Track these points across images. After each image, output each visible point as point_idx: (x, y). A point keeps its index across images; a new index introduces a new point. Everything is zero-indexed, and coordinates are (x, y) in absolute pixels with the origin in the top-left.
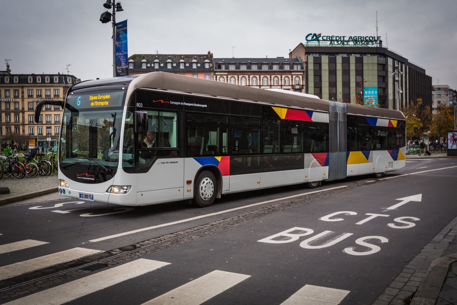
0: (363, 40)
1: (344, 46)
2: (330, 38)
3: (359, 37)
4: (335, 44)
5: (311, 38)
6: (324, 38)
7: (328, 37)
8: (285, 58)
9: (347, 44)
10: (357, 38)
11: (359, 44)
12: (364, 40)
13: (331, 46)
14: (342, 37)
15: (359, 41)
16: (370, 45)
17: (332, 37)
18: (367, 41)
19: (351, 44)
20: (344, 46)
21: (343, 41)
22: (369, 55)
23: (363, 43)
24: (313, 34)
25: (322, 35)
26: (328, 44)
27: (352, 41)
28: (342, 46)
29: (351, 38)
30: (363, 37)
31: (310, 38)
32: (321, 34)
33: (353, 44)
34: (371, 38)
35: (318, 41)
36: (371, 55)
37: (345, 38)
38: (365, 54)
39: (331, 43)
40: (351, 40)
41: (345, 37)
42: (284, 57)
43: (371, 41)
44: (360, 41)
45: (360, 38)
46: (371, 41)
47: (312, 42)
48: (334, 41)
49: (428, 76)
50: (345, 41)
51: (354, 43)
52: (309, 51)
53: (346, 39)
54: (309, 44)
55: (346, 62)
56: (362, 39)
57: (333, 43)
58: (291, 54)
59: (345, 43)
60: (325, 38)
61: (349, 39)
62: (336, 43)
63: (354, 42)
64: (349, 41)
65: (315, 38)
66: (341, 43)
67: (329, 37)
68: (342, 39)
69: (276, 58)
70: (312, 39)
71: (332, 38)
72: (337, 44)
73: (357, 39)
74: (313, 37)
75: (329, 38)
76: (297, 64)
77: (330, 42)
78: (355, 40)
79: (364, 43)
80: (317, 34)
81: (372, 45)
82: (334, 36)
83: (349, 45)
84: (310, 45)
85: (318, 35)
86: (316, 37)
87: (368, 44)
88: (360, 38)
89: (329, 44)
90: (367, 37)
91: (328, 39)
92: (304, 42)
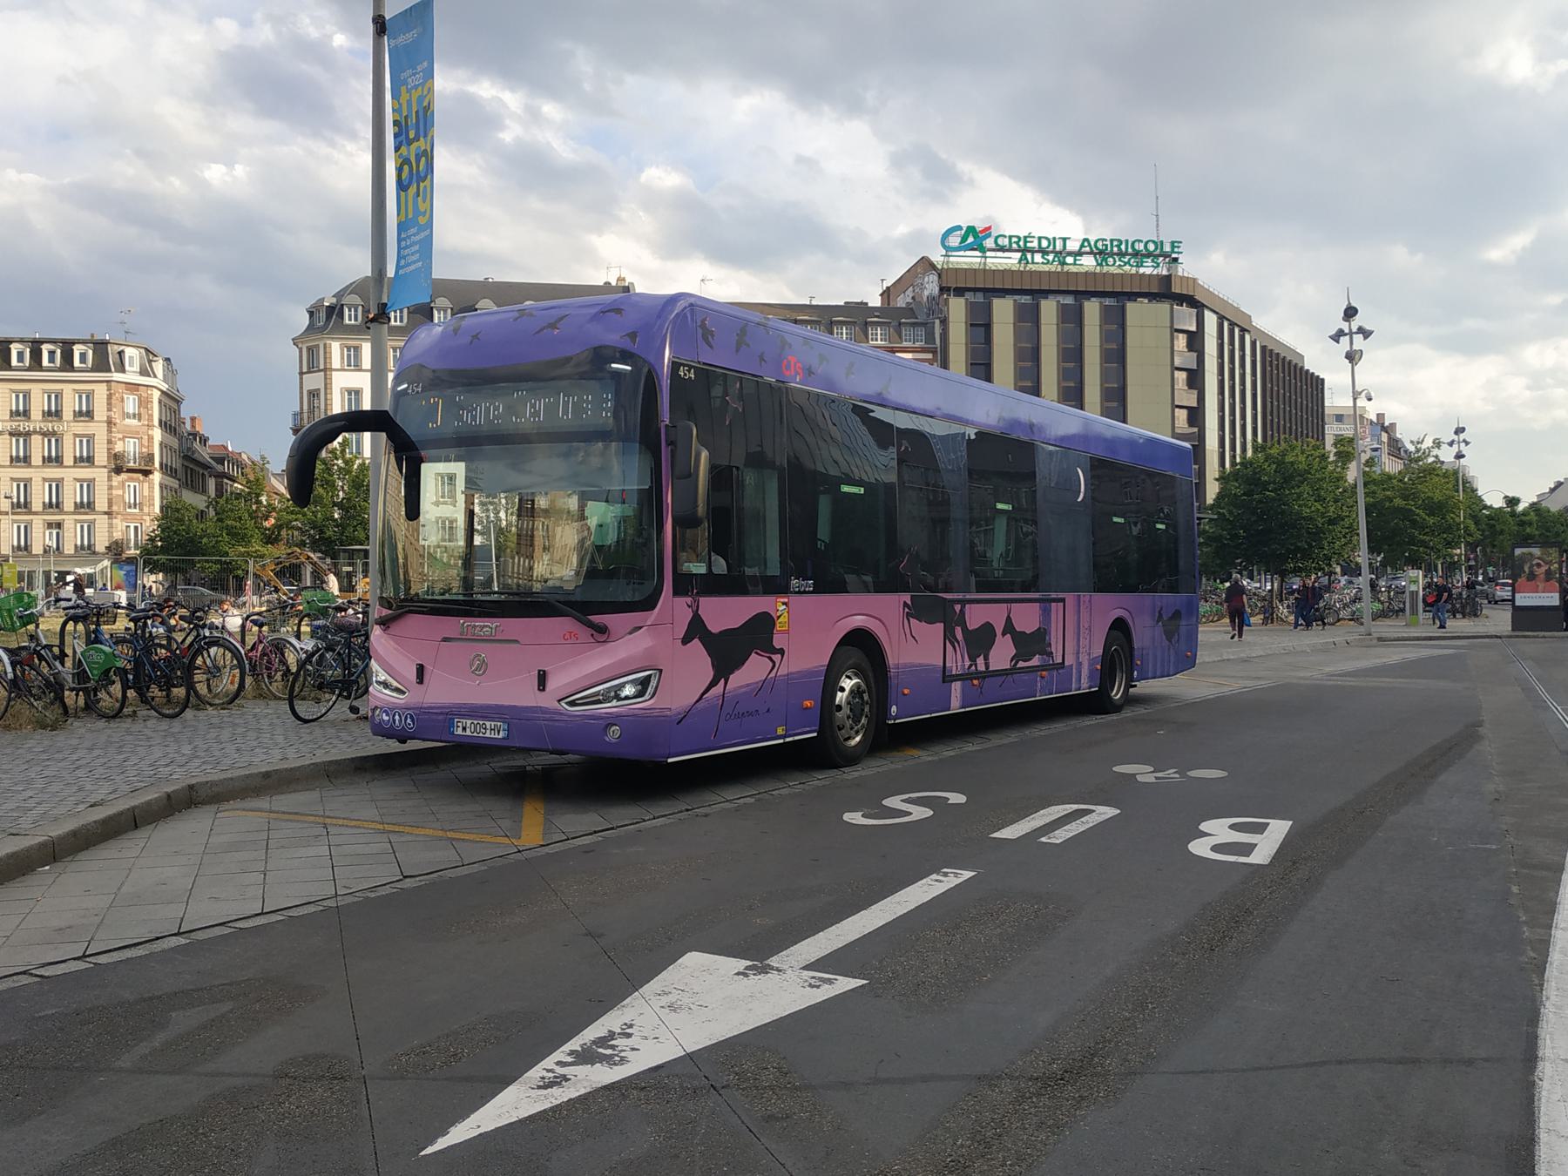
0: (1126, 254)
1: (1066, 268)
2: (1021, 243)
3: (1112, 241)
4: (1035, 261)
5: (959, 239)
6: (1000, 241)
7: (1014, 240)
8: (870, 305)
9: (1075, 264)
10: (1108, 243)
11: (1113, 265)
12: (1130, 250)
13: (1022, 269)
14: (1060, 238)
15: (1112, 254)
16: (1147, 269)
17: (1025, 237)
18: (1136, 254)
19: (1088, 262)
20: (1065, 270)
21: (1060, 253)
22: (1146, 301)
23: (1126, 260)
24: (965, 229)
25: (994, 234)
26: (1011, 261)
27: (1091, 253)
28: (1059, 269)
29: (1086, 244)
30: (1127, 241)
31: (954, 241)
32: (990, 228)
33: (1095, 264)
34: (1151, 247)
35: (983, 250)
36: (1150, 301)
37: (1068, 241)
38: (1133, 296)
39: (1023, 259)
40: (1088, 249)
41: (1069, 238)
42: (867, 304)
43: (1149, 255)
44: (1116, 254)
45: (1115, 243)
46: (1149, 255)
47: (962, 253)
48: (1033, 251)
49: (1313, 373)
50: (1070, 254)
51: (1097, 261)
52: (955, 284)
53: (1073, 246)
54: (951, 259)
55: (1072, 319)
56: (1123, 247)
57: (1030, 261)
58: (887, 294)
59: (1070, 260)
60: (1006, 242)
61: (1082, 246)
62: (1038, 258)
63: (1098, 256)
64: (1079, 253)
65: (971, 239)
66: (1054, 261)
67: (1016, 240)
68: (1059, 247)
69: (842, 304)
70: (961, 243)
71: (1025, 242)
72: (1043, 263)
73: (1106, 245)
74: (964, 239)
75: (1017, 243)
76: (914, 325)
77: (1018, 255)
78: (1101, 254)
79: (1129, 260)
80: (980, 226)
81: (1155, 267)
82: (1034, 237)
83: (1082, 265)
84: (952, 263)
85: (982, 232)
86: (975, 237)
87: (1142, 266)
88: (1115, 243)
89: (1017, 261)
90: (1140, 241)
91: (1014, 246)
92: (937, 257)
